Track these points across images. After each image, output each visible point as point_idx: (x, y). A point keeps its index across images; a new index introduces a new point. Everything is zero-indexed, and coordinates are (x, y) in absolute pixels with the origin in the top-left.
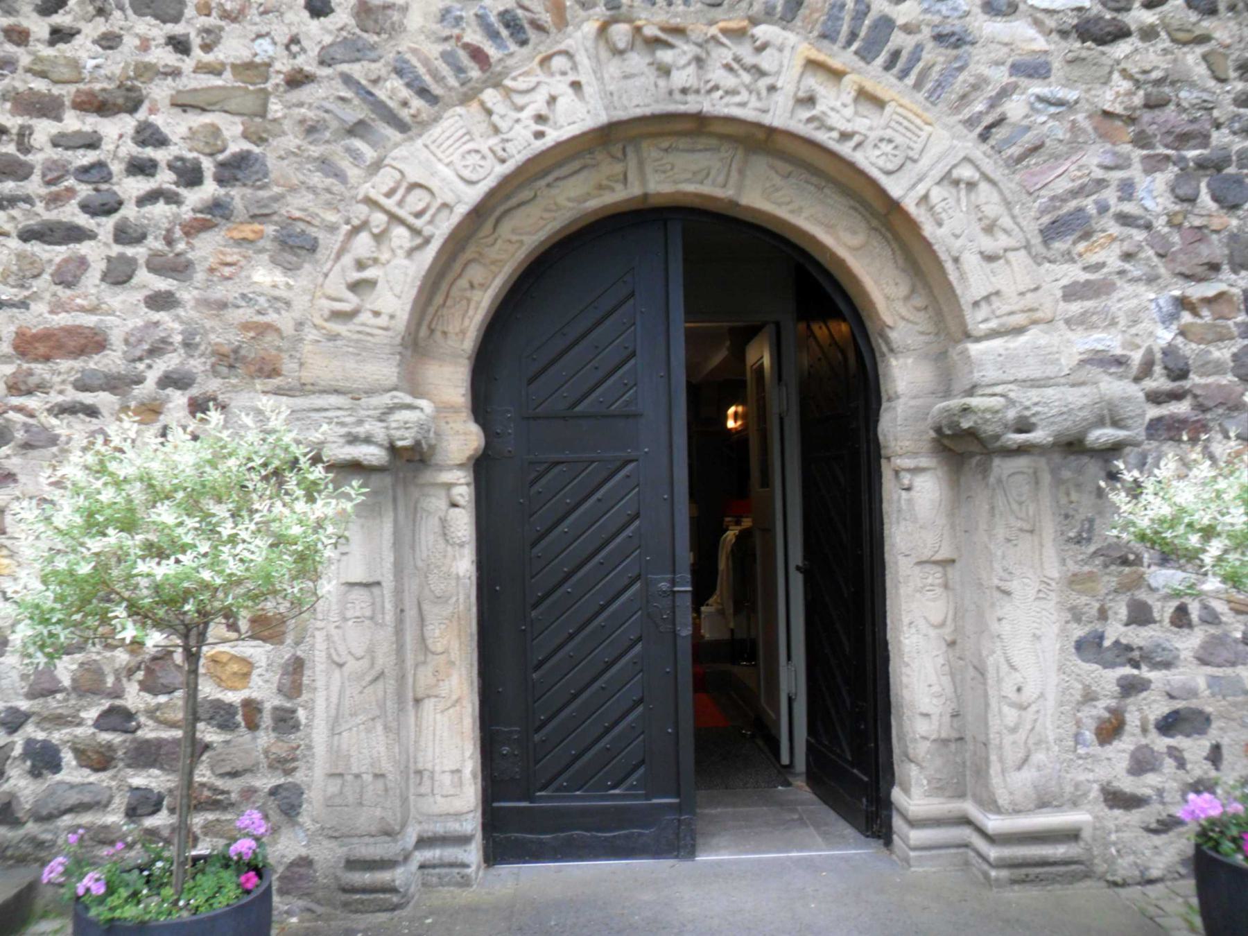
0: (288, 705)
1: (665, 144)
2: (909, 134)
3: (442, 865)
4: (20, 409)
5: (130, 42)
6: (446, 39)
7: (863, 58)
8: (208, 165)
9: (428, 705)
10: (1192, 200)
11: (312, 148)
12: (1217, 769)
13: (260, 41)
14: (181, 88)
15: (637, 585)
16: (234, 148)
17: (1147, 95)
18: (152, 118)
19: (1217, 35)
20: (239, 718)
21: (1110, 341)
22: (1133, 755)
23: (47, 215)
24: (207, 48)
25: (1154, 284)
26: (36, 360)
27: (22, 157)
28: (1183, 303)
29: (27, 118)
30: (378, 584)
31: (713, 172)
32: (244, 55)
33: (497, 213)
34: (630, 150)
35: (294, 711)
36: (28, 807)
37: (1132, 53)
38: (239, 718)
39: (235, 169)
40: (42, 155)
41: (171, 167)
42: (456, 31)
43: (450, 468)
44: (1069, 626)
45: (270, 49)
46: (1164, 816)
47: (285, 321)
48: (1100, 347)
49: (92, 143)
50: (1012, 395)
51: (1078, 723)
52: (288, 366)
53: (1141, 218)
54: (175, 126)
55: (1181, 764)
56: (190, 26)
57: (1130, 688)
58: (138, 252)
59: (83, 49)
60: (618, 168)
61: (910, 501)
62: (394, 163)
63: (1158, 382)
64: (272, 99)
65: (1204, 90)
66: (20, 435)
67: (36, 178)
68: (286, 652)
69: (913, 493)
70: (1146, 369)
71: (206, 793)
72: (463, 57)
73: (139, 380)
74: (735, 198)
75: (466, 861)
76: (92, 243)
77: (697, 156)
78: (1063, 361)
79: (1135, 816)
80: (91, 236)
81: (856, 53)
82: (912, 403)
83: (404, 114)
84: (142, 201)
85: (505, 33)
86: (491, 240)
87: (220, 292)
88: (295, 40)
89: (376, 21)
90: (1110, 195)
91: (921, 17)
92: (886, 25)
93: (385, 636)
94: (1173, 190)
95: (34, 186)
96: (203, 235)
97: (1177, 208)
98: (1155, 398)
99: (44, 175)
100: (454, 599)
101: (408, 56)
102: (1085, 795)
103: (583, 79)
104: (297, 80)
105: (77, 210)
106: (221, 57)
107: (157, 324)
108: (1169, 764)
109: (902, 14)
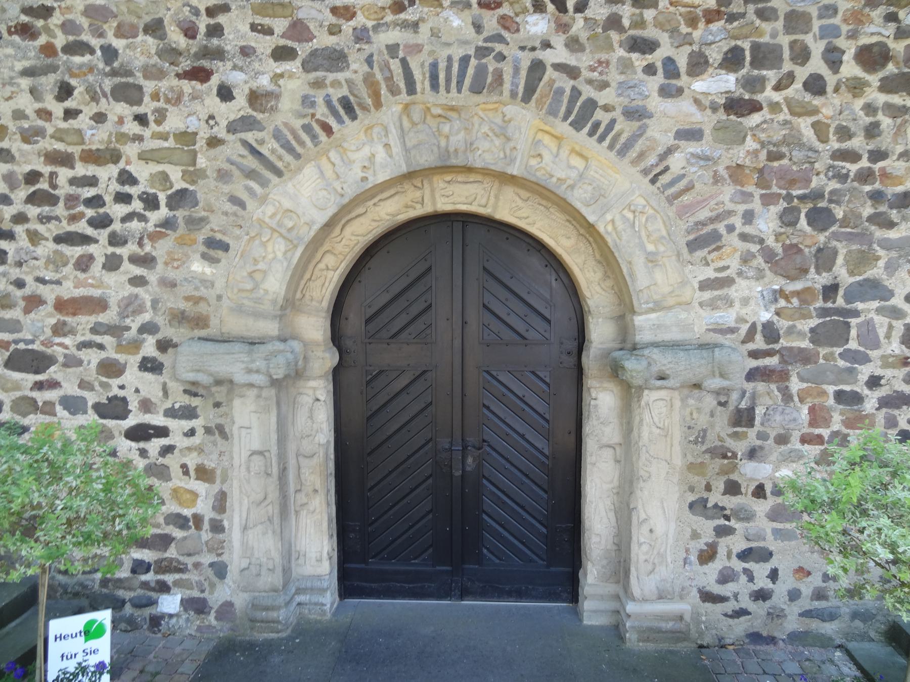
0: (218, 518)
1: (448, 178)
2: (602, 179)
3: (310, 603)
4: (60, 345)
5: (112, 118)
6: (305, 116)
7: (576, 129)
8: (162, 198)
9: (303, 513)
10: (793, 223)
11: (225, 187)
12: (774, 583)
13: (190, 118)
14: (143, 148)
15: (430, 445)
16: (179, 185)
17: (769, 153)
18: (128, 168)
19: (824, 110)
20: (191, 524)
21: (728, 317)
22: (720, 572)
23: (66, 227)
24: (159, 122)
25: (761, 281)
26: (67, 314)
27: (52, 192)
28: (781, 293)
29: (53, 167)
31: (479, 197)
32: (182, 127)
33: (343, 222)
34: (425, 182)
35: (221, 521)
37: (762, 123)
38: (191, 524)
39: (179, 199)
40: (64, 189)
41: (140, 197)
42: (311, 111)
43: (314, 379)
44: (686, 494)
45: (196, 122)
46: (737, 608)
47: (211, 294)
48: (721, 321)
49: (92, 181)
50: (654, 356)
51: (687, 551)
52: (214, 322)
53: (756, 236)
54: (143, 172)
55: (751, 579)
56: (147, 107)
57: (722, 532)
58: (124, 251)
59: (83, 122)
60: (418, 194)
61: (596, 406)
62: (275, 197)
63: (759, 343)
64: (199, 156)
65: (811, 149)
66: (61, 359)
67: (61, 204)
68: (216, 488)
69: (597, 402)
70: (750, 336)
71: (174, 564)
72: (317, 128)
73: (128, 328)
74: (492, 214)
75: (324, 602)
76: (96, 245)
77: (469, 186)
78: (696, 329)
79: (719, 608)
80: (96, 241)
81: (570, 124)
82: (600, 346)
83: (279, 164)
84: (124, 220)
85: (342, 112)
86: (339, 239)
87: (172, 274)
88: (212, 117)
89: (261, 104)
90: (737, 221)
91: (616, 100)
92: (591, 105)
93: (274, 481)
94: (781, 218)
95: (60, 210)
96: (161, 241)
97: (783, 230)
98: (754, 354)
99: (65, 204)
101: (282, 128)
102: (688, 594)
103: (392, 144)
104: (214, 142)
105: (86, 225)
106: (167, 129)
107: (137, 296)
108: (743, 578)
109: (604, 97)
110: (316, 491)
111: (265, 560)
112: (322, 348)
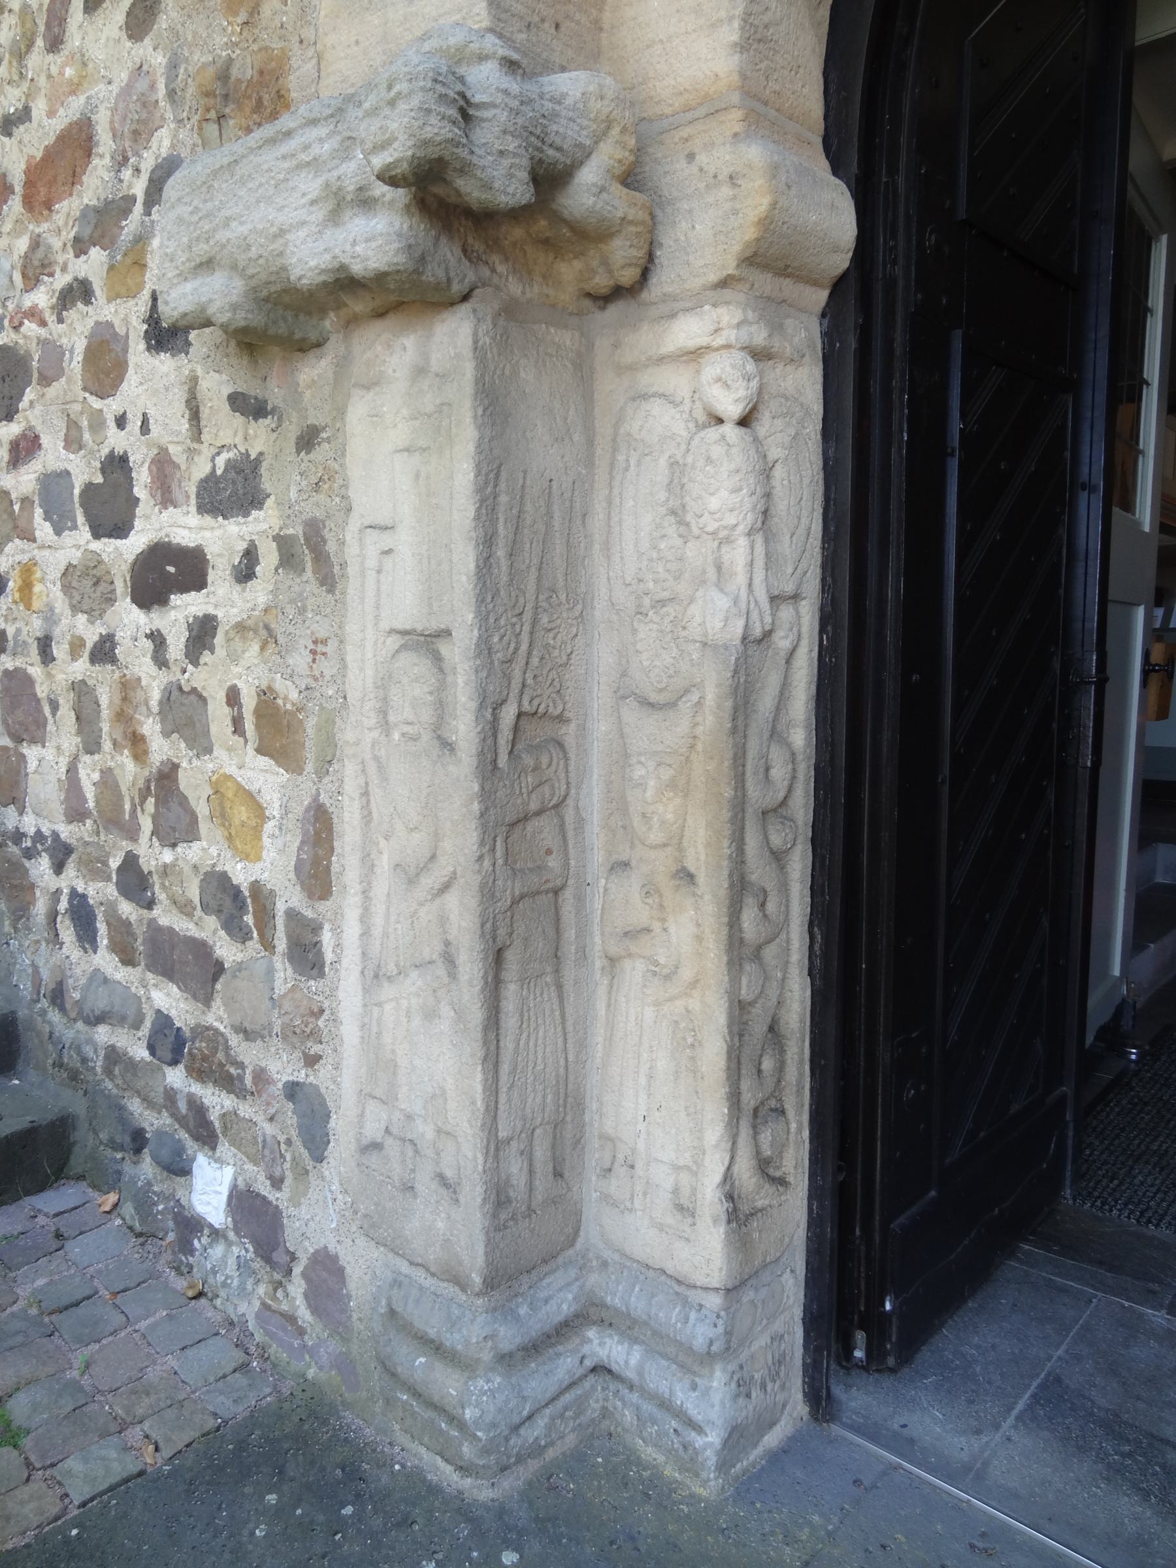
0: (309, 914)
9: (634, 971)
30: (447, 633)
36: (76, 995)
38: (249, 919)
100: (694, 697)
110: (686, 877)
111: (430, 1134)
112: (733, 121)
